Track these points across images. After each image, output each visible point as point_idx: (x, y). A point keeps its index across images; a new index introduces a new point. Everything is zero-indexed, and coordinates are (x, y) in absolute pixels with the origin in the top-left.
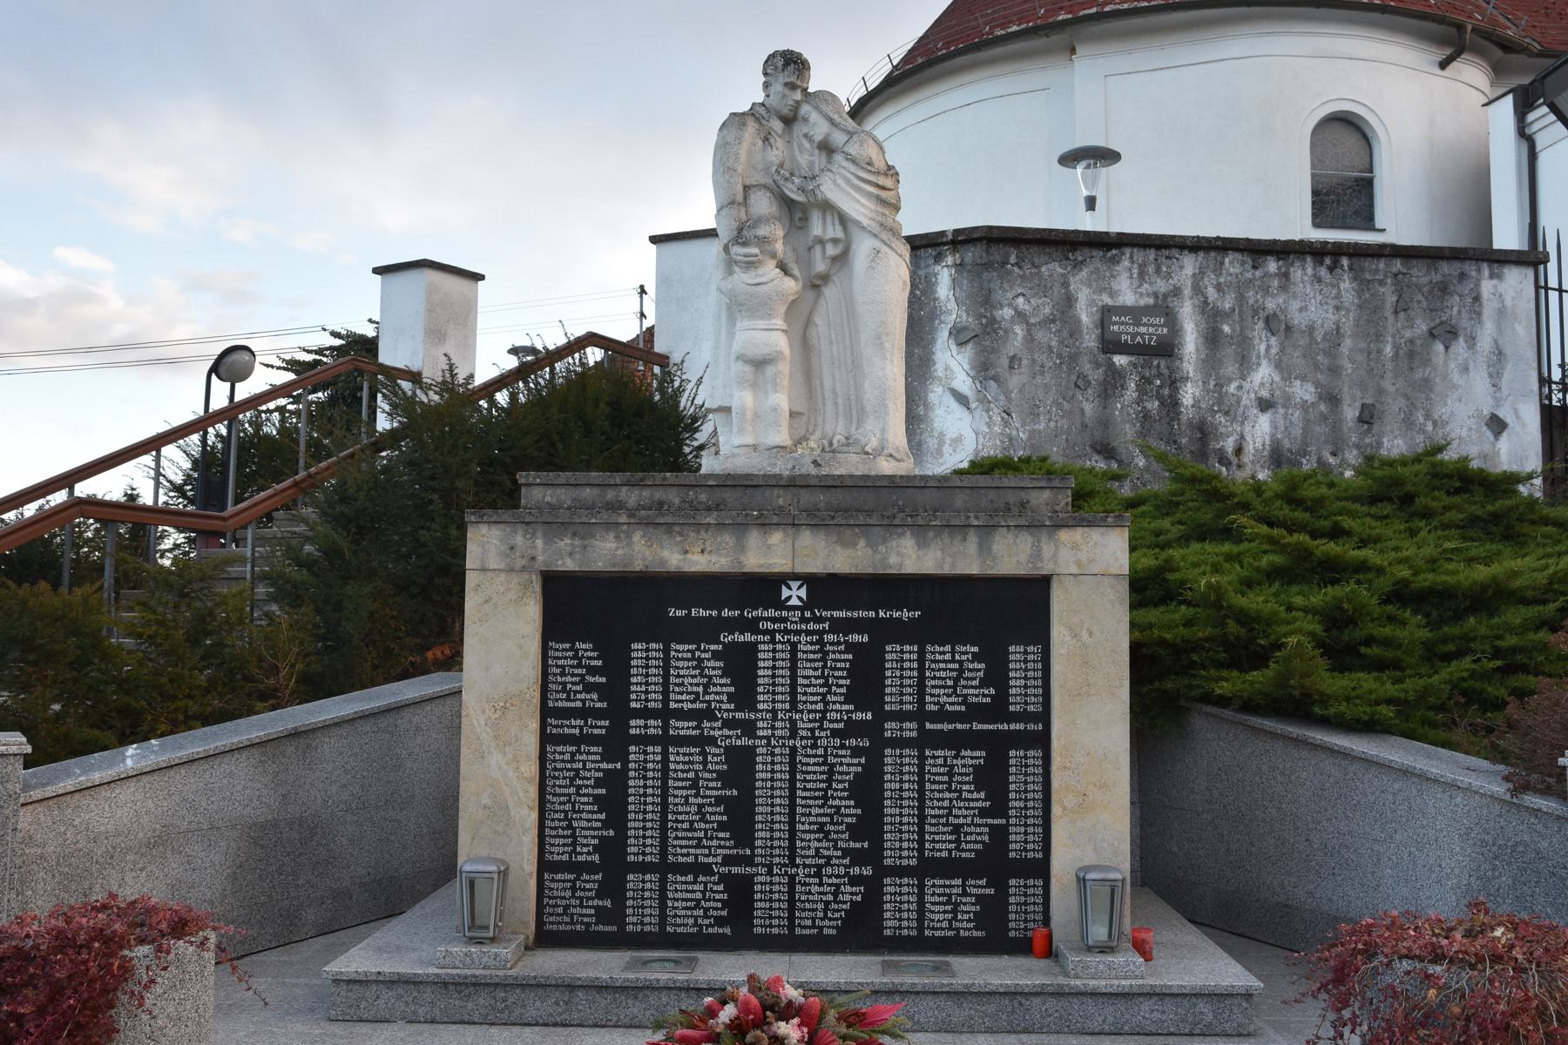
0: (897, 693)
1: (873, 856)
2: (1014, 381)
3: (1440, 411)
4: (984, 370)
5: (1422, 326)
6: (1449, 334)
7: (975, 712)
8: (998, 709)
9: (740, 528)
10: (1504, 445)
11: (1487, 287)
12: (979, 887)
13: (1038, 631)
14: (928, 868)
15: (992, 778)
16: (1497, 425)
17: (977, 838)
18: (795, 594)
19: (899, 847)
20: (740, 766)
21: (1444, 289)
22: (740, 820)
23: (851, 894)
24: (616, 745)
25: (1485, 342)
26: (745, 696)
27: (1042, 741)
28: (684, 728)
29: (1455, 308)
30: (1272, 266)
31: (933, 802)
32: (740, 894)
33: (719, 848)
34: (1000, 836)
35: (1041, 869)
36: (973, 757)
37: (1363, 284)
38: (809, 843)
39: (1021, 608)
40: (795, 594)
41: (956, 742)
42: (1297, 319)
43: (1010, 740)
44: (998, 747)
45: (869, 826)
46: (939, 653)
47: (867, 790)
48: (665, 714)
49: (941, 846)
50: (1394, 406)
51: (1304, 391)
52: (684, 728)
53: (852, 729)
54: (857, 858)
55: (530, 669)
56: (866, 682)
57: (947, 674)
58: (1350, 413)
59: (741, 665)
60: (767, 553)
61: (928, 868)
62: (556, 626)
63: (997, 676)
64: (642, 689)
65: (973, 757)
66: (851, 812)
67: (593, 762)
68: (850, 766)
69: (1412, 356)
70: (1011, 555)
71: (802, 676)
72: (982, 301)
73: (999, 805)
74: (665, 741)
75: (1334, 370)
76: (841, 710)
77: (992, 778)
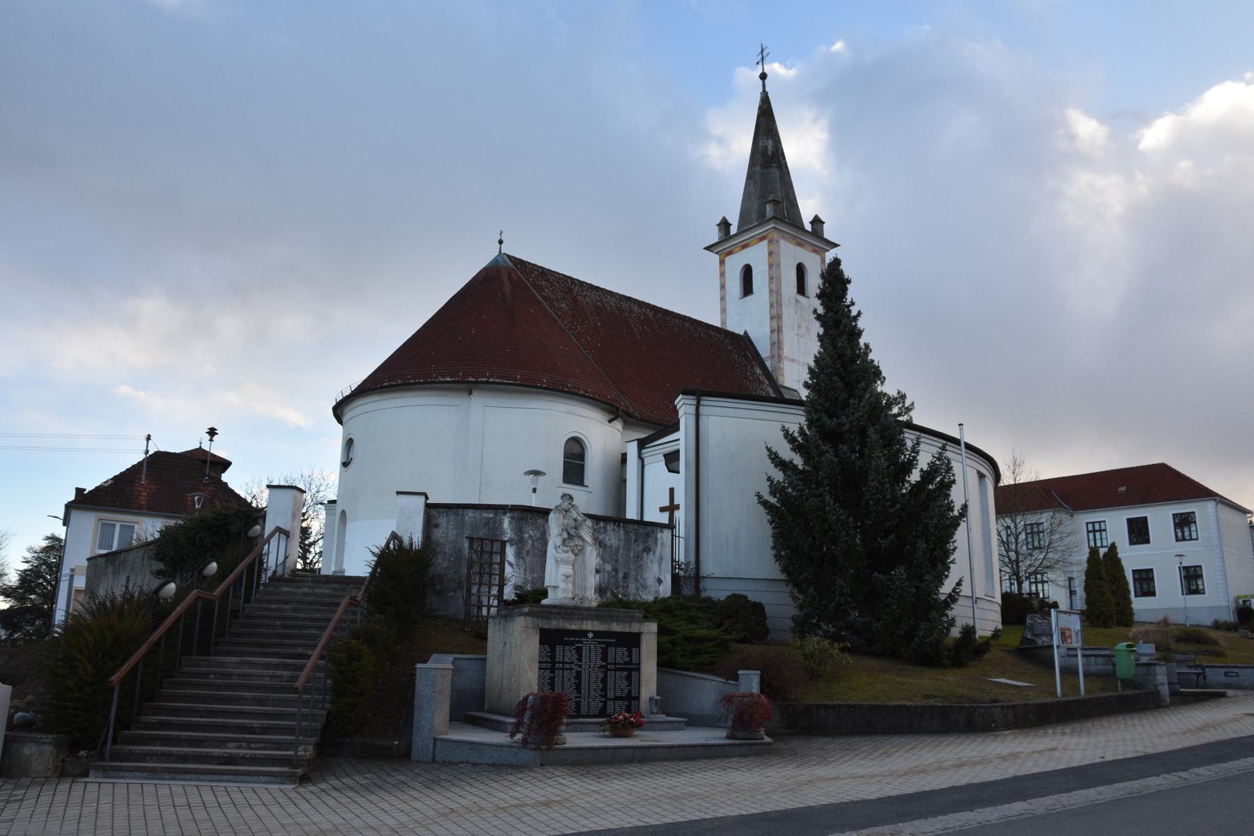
0: (611, 659)
1: (605, 696)
2: (528, 559)
3: (645, 576)
4: (518, 555)
5: (641, 547)
6: (647, 550)
7: (626, 663)
8: (630, 663)
9: (582, 619)
10: (661, 588)
11: (659, 535)
12: (626, 703)
13: (638, 645)
14: (616, 699)
15: (629, 678)
16: (660, 581)
17: (625, 692)
18: (591, 635)
19: (610, 694)
20: (579, 674)
21: (648, 535)
22: (578, 688)
23: (601, 705)
24: (553, 670)
25: (658, 554)
26: (580, 659)
27: (638, 670)
28: (567, 666)
29: (650, 543)
30: (602, 524)
31: (617, 684)
32: (578, 705)
33: (575, 694)
34: (630, 691)
35: (638, 698)
36: (625, 673)
37: (626, 532)
38: (593, 693)
39: (633, 641)
40: (591, 635)
41: (622, 670)
42: (608, 543)
43: (632, 669)
44: (630, 671)
45: (604, 689)
46: (619, 649)
47: (604, 681)
48: (563, 663)
49: (619, 694)
50: (633, 573)
51: (608, 567)
52: (567, 666)
53: (602, 667)
54: (602, 696)
55: (537, 652)
56: (604, 658)
57: (618, 654)
58: (621, 575)
59: (579, 651)
60: (588, 625)
61: (616, 699)
62: (542, 642)
63: (630, 655)
64: (559, 657)
65: (625, 673)
66: (601, 686)
67: (548, 674)
68: (601, 675)
69: (638, 557)
70: (635, 628)
71: (592, 653)
72: (519, 531)
73: (630, 685)
74: (563, 669)
75: (617, 561)
76: (599, 662)
77: (629, 678)
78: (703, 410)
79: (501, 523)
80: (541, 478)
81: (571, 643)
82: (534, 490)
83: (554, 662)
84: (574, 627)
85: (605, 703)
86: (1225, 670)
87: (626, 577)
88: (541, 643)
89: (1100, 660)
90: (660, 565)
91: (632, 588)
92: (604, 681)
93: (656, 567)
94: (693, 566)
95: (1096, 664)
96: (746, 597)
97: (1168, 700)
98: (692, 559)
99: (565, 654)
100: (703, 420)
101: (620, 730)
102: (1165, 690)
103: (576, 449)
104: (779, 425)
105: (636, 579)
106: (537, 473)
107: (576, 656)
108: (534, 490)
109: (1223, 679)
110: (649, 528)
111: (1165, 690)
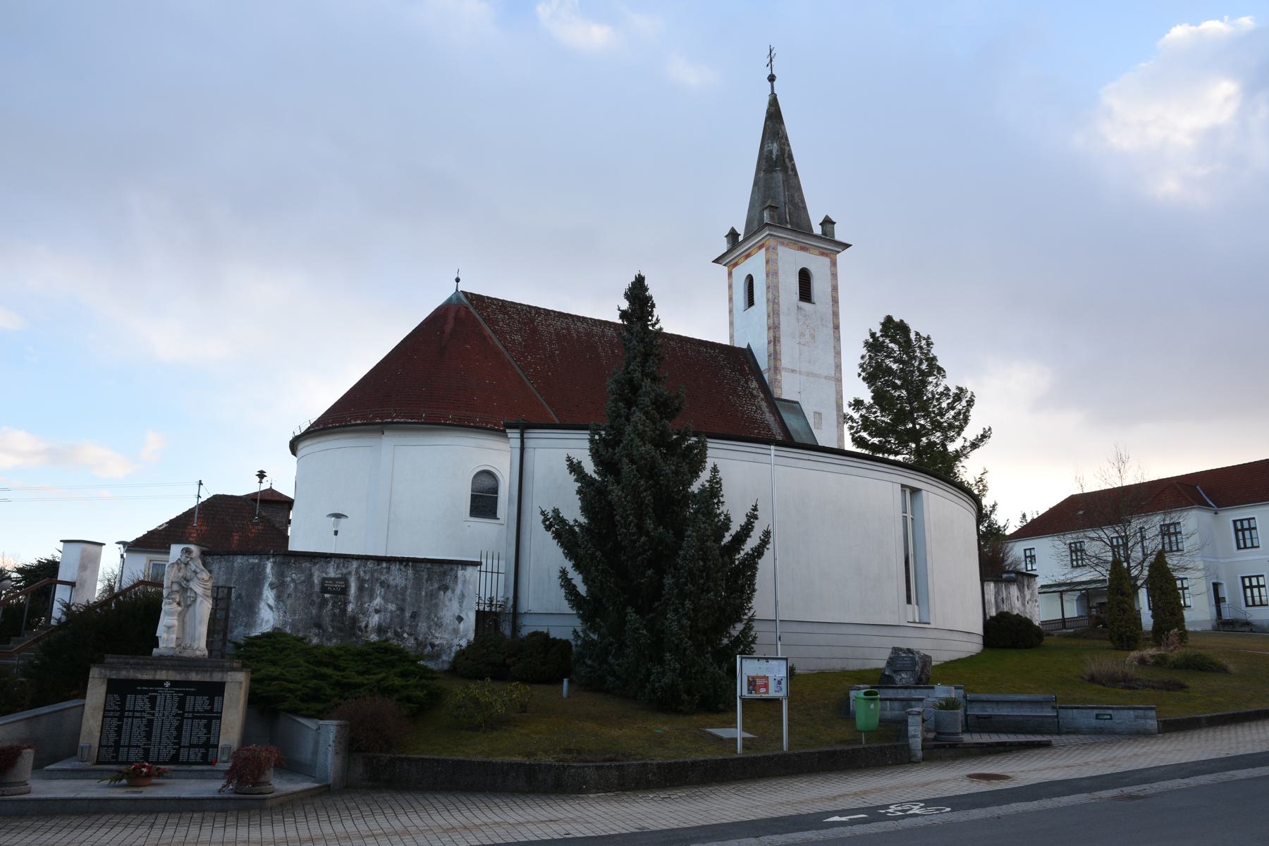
0: (188, 707)
1: (179, 743)
2: (289, 602)
3: (441, 614)
4: (279, 598)
5: (436, 586)
6: (445, 588)
7: (206, 711)
8: (211, 711)
9: (156, 670)
10: (462, 626)
11: (460, 573)
12: (203, 750)
13: (222, 694)
14: (191, 746)
15: (208, 727)
16: (460, 619)
17: (204, 739)
18: (167, 684)
19: (185, 741)
20: (150, 723)
21: (445, 573)
22: (149, 735)
23: (173, 752)
24: (121, 718)
25: (458, 592)
26: (153, 708)
27: (220, 718)
28: (138, 714)
29: (448, 580)
30: (384, 565)
31: (194, 731)
32: (147, 751)
33: (144, 741)
34: (208, 739)
35: (217, 746)
36: (204, 721)
37: (416, 571)
38: (164, 740)
39: (217, 689)
40: (167, 684)
41: (200, 718)
42: (392, 583)
43: (212, 718)
44: (210, 719)
45: (179, 737)
46: (199, 698)
47: (179, 729)
48: (134, 711)
49: (195, 741)
50: (424, 612)
51: (392, 607)
52: (138, 714)
53: (177, 715)
54: (175, 744)
55: (102, 701)
56: (181, 705)
57: (201, 703)
58: (408, 614)
59: (153, 701)
60: (162, 675)
61: (191, 746)
62: (109, 691)
63: (212, 704)
64: (129, 706)
65: (204, 721)
66: (175, 733)
67: (115, 722)
68: (176, 723)
69: (432, 595)
70: (217, 677)
71: (167, 704)
72: (280, 575)
73: (209, 732)
74: (133, 717)
75: (404, 600)
76: (175, 710)
77: (208, 727)
78: (528, 443)
79: (264, 568)
80: (343, 520)
81: (143, 692)
82: (336, 533)
83: (123, 710)
84: (145, 677)
85: (178, 751)
86: (1096, 712)
87: (414, 616)
88: (108, 692)
89: (896, 704)
90: (461, 603)
91: (422, 626)
92: (179, 729)
93: (455, 604)
94: (511, 602)
95: (892, 709)
96: (546, 636)
97: (920, 754)
98: (511, 595)
99: (137, 702)
100: (529, 454)
101: (136, 779)
102: (916, 743)
103: (487, 482)
104: (562, 455)
105: (428, 618)
106: (338, 516)
107: (148, 705)
108: (336, 533)
109: (1094, 722)
110: (446, 566)
111: (916, 743)
